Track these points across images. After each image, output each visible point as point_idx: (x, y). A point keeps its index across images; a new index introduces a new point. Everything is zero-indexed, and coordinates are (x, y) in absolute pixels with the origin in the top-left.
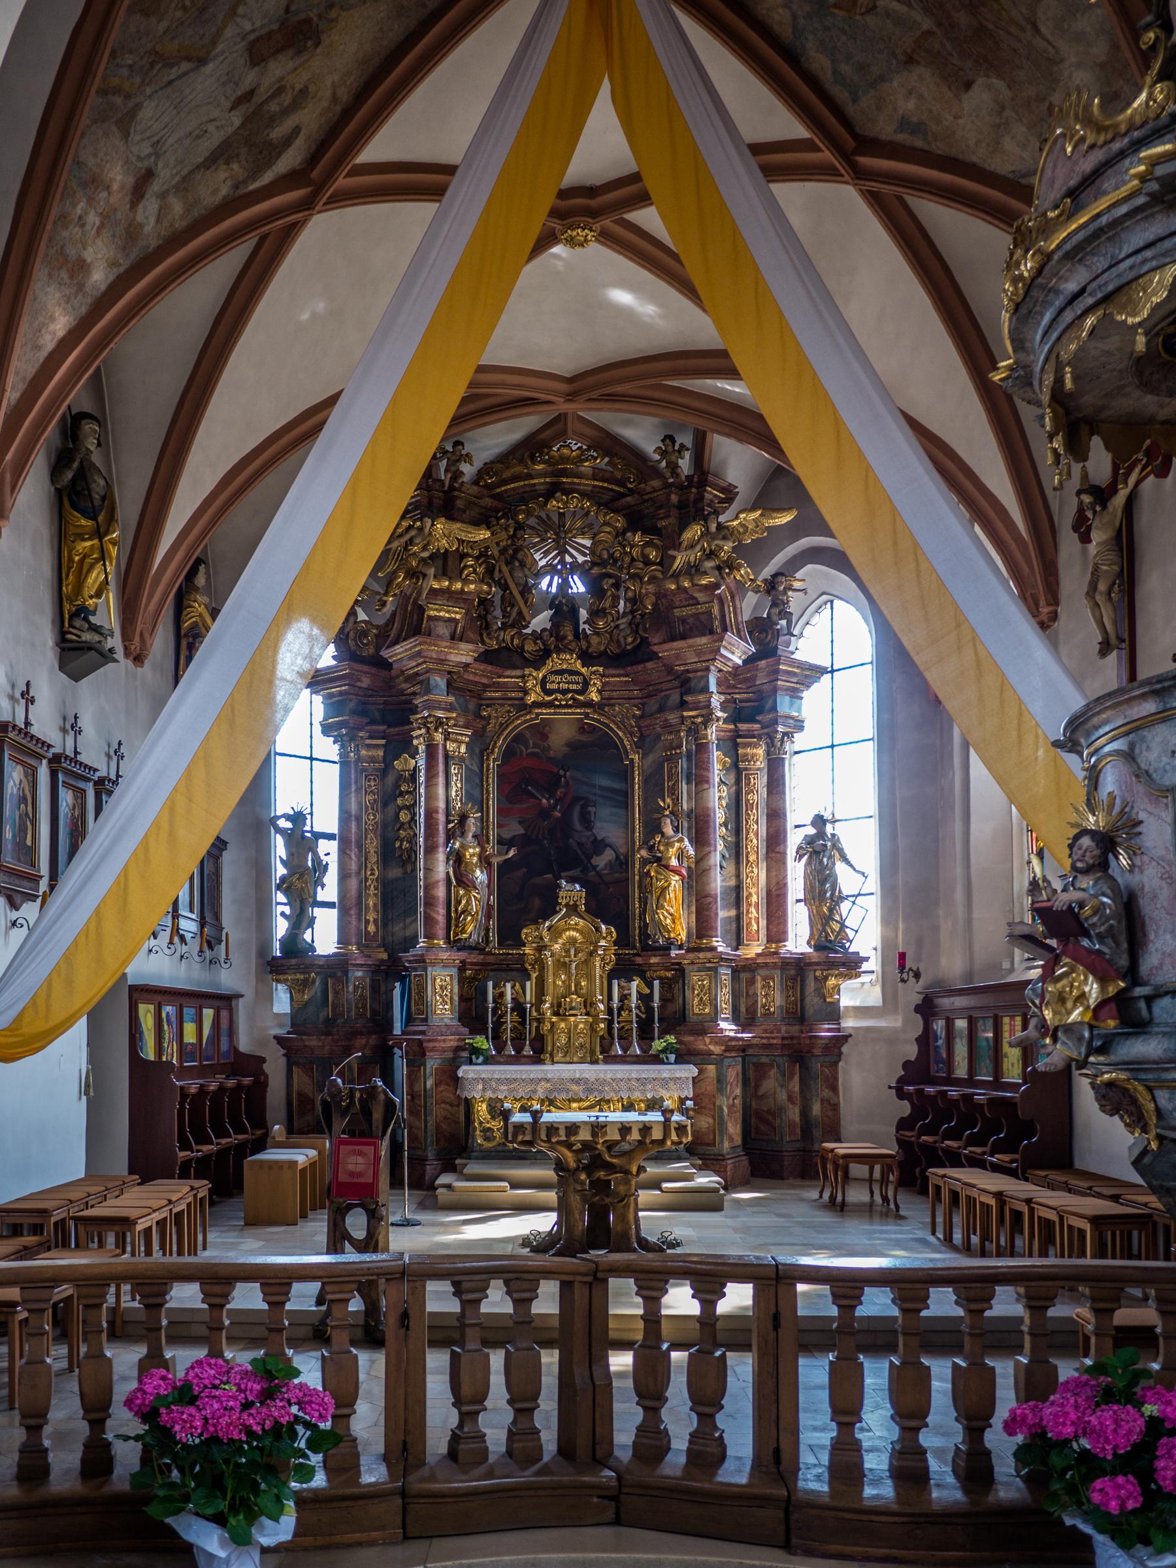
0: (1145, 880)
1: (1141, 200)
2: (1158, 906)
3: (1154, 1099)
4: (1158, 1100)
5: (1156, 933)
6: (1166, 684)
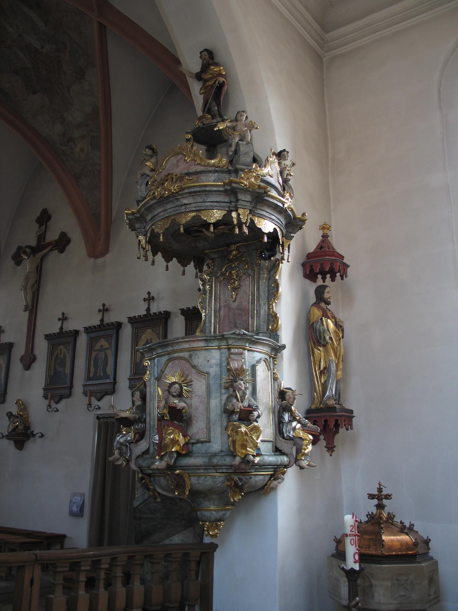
1: (221, 189)
3: (190, 480)
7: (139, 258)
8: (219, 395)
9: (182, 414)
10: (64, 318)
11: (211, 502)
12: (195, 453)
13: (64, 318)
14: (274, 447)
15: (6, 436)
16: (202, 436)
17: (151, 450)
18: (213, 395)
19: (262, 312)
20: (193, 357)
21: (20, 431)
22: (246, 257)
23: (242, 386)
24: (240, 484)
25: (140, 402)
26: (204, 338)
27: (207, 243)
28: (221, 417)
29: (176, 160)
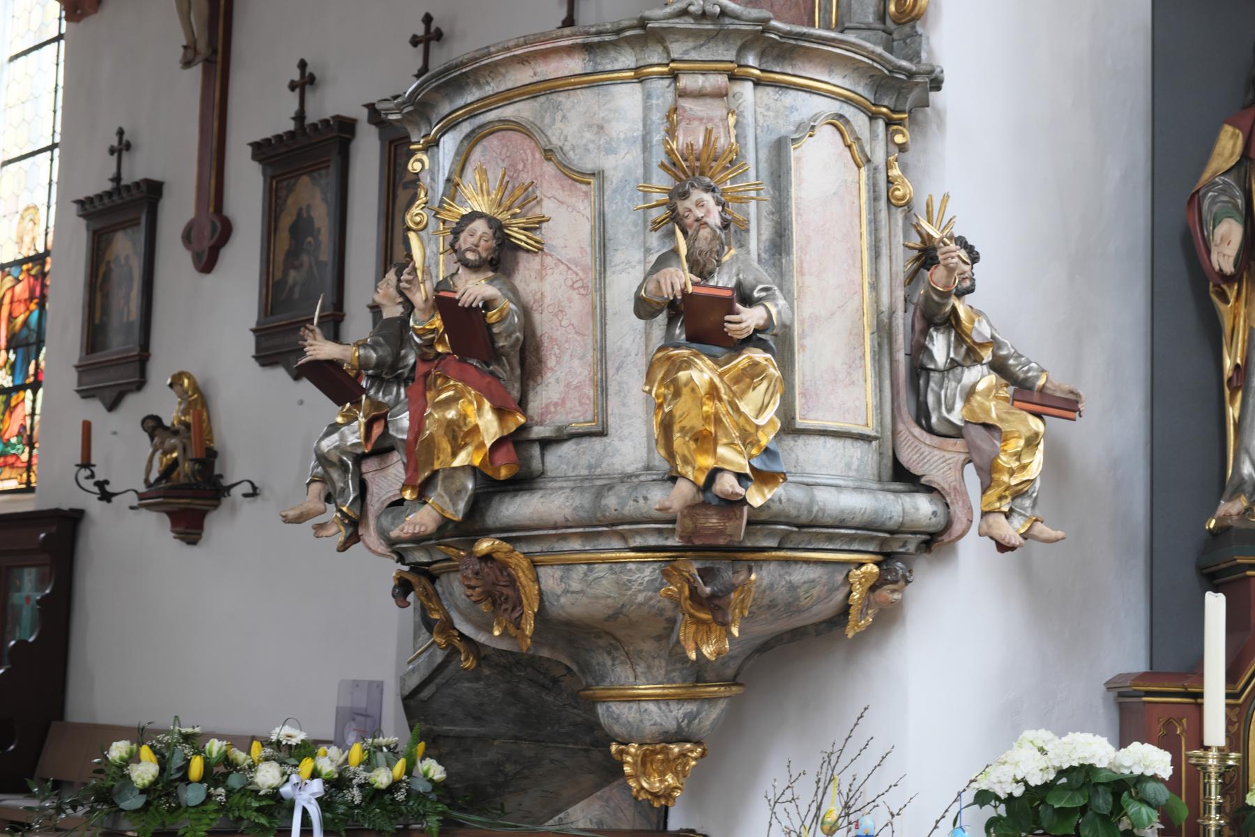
0: (547, 287)
2: (564, 323)
3: (537, 580)
4: (542, 580)
5: (558, 358)
6: (607, 38)
9: (489, 326)
10: (305, 82)
11: (640, 669)
12: (554, 479)
13: (305, 82)
14: (888, 462)
15: (141, 496)
16: (577, 415)
21: (182, 480)
23: (708, 212)
24: (708, 590)
26: (580, 41)
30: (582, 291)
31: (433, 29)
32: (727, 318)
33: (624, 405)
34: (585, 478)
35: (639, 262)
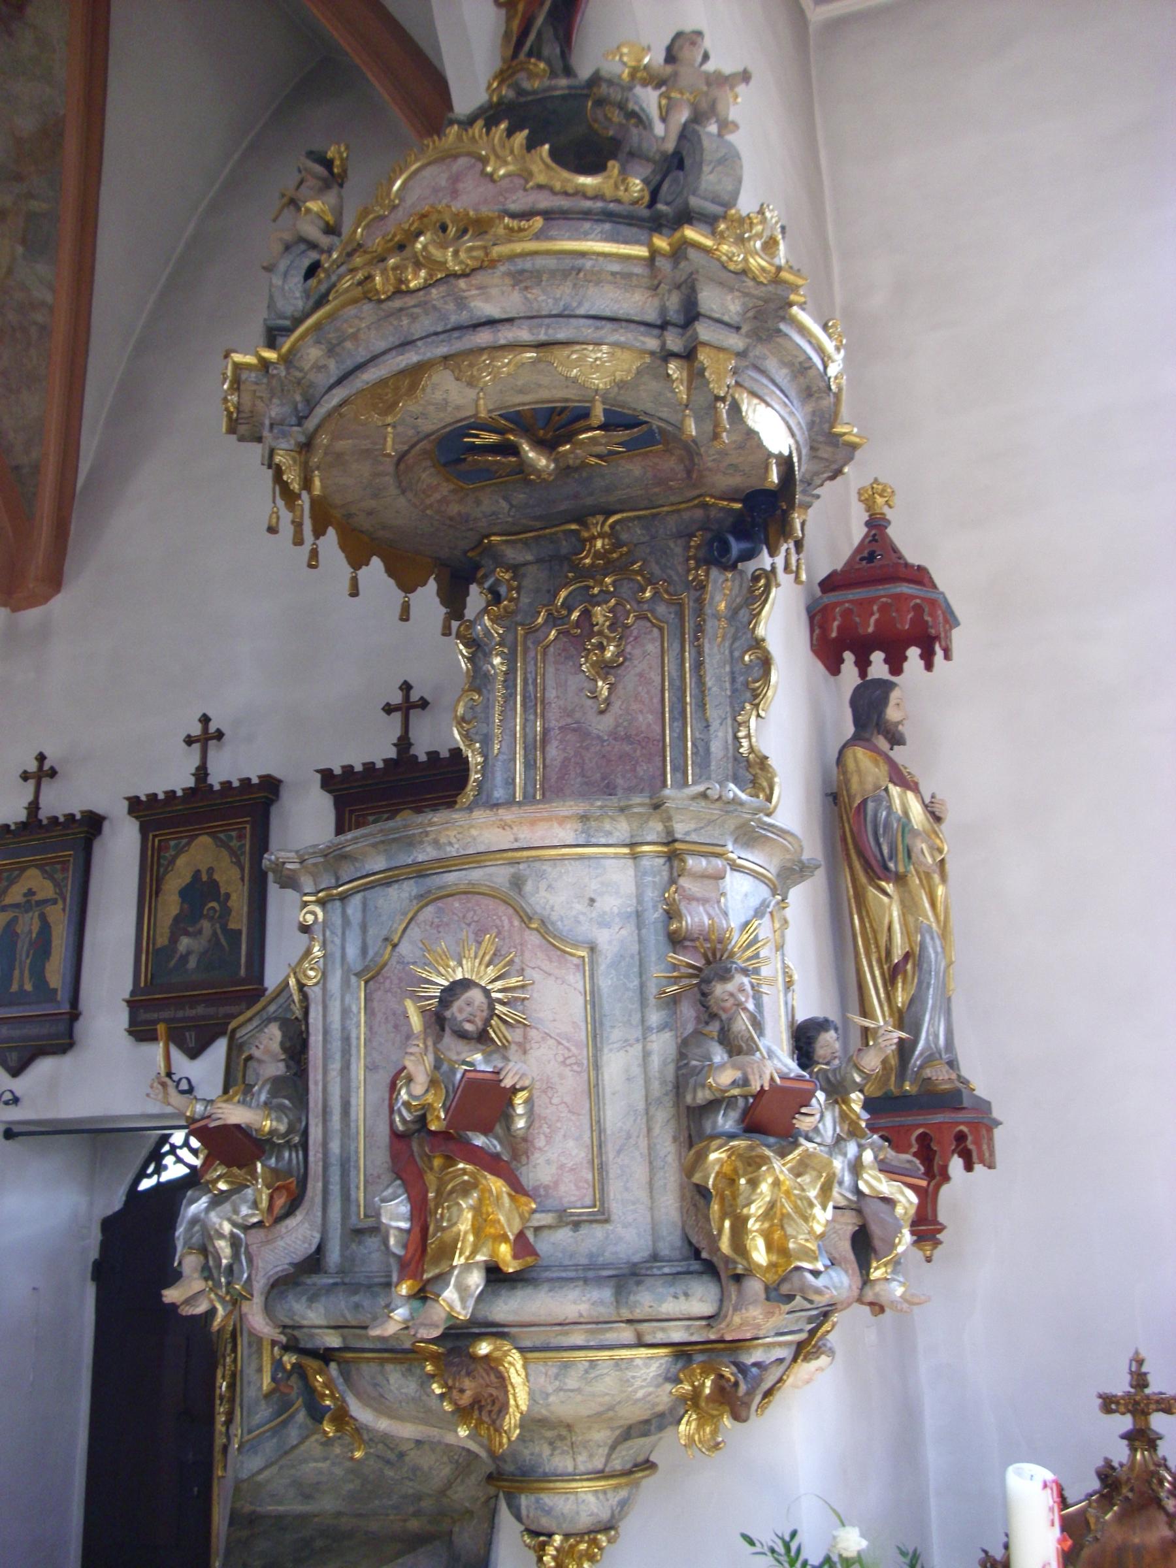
2: (555, 1101)
5: (549, 1139)
7: (272, 530)
8: (638, 1033)
17: (334, 1256)
18: (615, 1034)
19: (716, 747)
20: (528, 887)
22: (645, 561)
25: (282, 1065)
27: (504, 504)
28: (649, 1119)
29: (445, 176)
30: (575, 1067)
31: (46, 767)
32: (803, 1110)
33: (627, 1189)
34: (587, 1268)
35: (637, 1040)
